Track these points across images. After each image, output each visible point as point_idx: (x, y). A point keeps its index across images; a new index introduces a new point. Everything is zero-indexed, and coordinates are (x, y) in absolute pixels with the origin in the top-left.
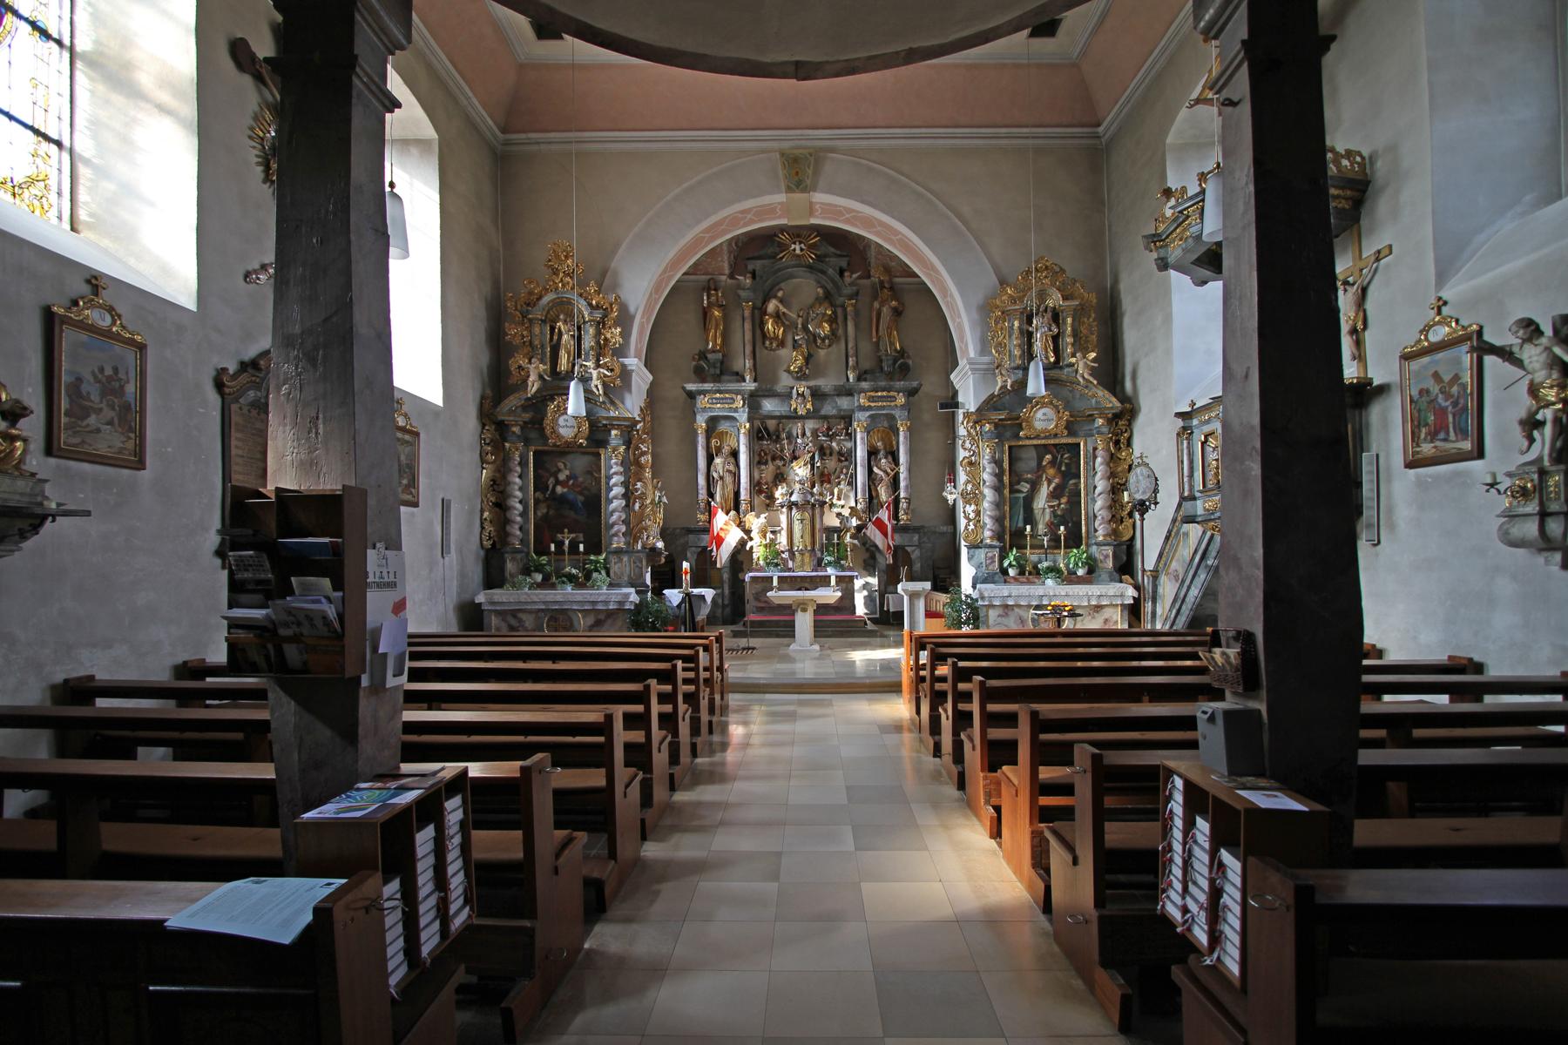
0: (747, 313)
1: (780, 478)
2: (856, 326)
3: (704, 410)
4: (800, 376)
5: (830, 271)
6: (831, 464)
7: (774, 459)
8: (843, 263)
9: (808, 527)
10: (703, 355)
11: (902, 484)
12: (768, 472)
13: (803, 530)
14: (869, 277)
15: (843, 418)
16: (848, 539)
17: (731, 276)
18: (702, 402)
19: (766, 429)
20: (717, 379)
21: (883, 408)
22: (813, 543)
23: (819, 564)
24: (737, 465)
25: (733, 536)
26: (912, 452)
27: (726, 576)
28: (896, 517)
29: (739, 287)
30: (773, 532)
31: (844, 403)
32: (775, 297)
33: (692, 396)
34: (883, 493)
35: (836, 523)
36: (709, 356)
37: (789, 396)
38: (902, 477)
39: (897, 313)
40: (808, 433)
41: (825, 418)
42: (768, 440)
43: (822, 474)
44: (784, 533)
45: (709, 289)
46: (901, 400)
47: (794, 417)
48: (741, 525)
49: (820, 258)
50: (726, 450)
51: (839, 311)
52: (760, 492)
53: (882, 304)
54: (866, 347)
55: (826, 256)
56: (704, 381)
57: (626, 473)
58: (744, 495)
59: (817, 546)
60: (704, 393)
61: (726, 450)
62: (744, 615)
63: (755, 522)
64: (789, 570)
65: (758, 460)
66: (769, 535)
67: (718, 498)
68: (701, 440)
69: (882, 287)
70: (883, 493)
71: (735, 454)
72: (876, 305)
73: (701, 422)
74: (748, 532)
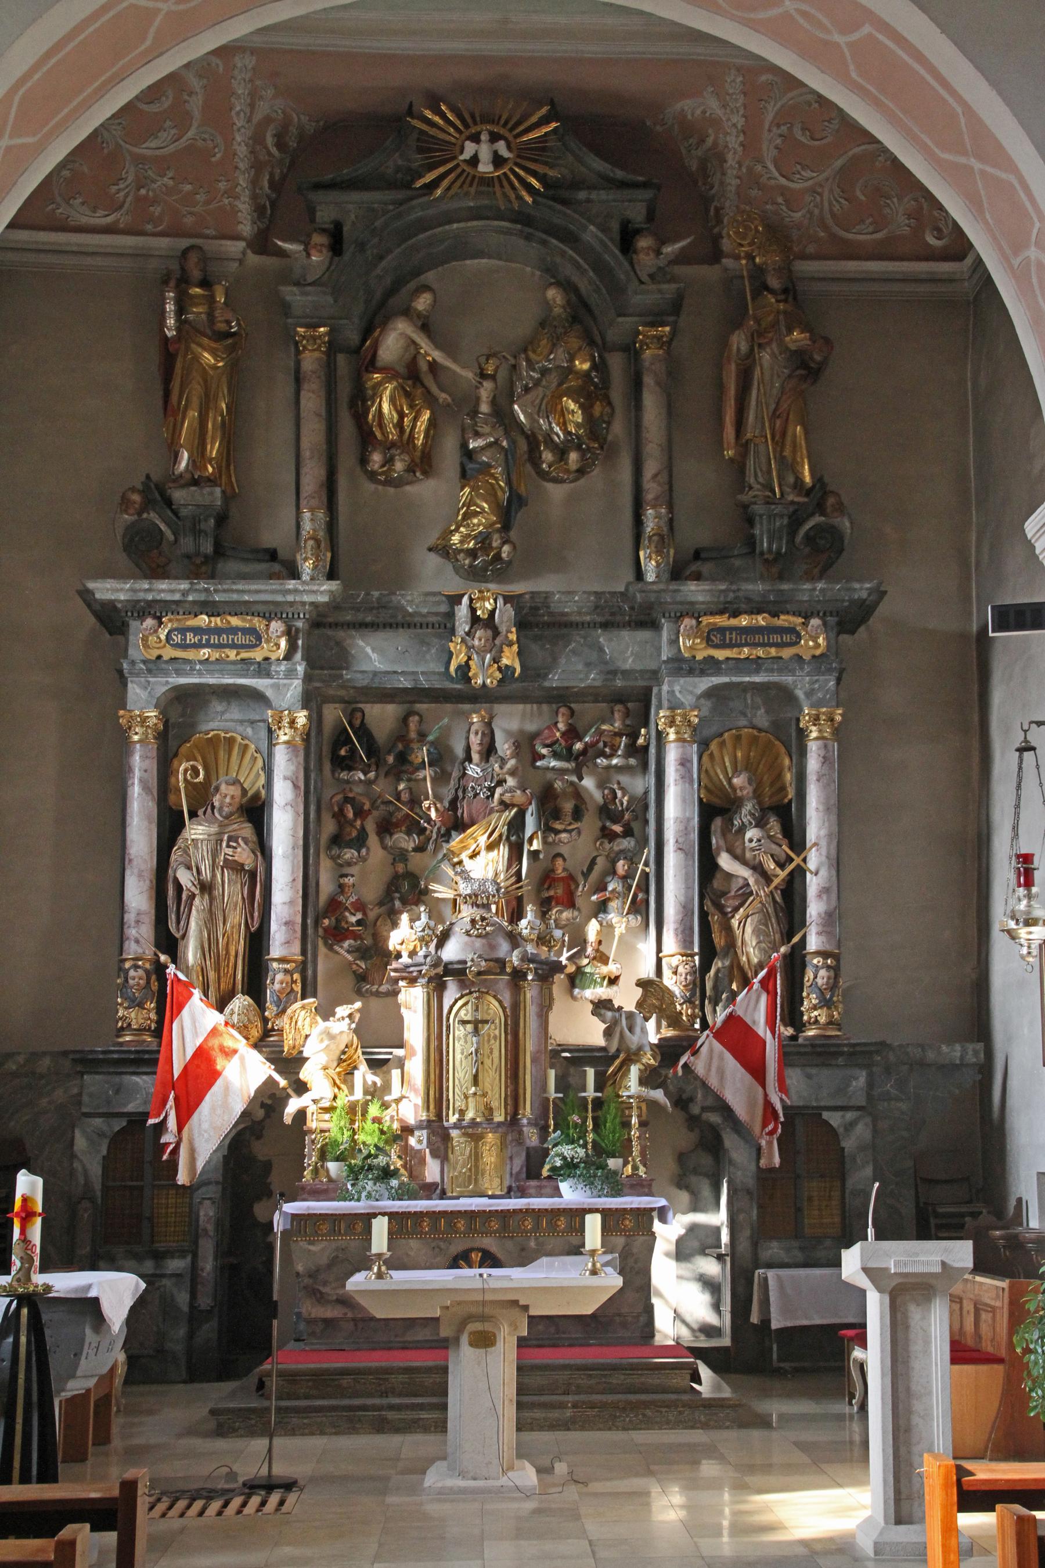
0: (310, 361)
1: (407, 890)
2: (671, 411)
3: (155, 666)
4: (483, 565)
5: (591, 234)
6: (577, 844)
7: (386, 828)
8: (637, 213)
9: (497, 1052)
10: (157, 494)
11: (815, 909)
12: (369, 869)
13: (478, 1056)
14: (715, 256)
15: (619, 698)
16: (632, 1085)
17: (261, 244)
18: (149, 639)
20: (203, 567)
21: (756, 664)
22: (514, 1100)
23: (533, 1171)
24: (263, 848)
25: (245, 1073)
26: (844, 810)
27: (207, 1213)
28: (793, 1016)
29: (286, 277)
30: (375, 1065)
31: (626, 649)
32: (407, 312)
33: (113, 621)
34: (751, 939)
35: (592, 1033)
36: (179, 495)
37: (446, 626)
38: (813, 884)
39: (807, 368)
40: (504, 747)
41: (561, 698)
42: (373, 777)
43: (546, 878)
44: (416, 1067)
45: (183, 282)
46: (815, 640)
47: (463, 694)
48: (266, 1040)
49: (556, 191)
50: (226, 796)
51: (616, 362)
52: (337, 934)
53: (757, 341)
54: (700, 478)
55: (576, 184)
56: (158, 572)
58: (281, 942)
59: (527, 1111)
60: (155, 610)
61: (226, 796)
62: (263, 1348)
63: (321, 1036)
64: (430, 1190)
65: (333, 829)
66: (363, 1076)
67: (191, 953)
68: (141, 764)
69: (761, 287)
70: (751, 939)
71: (255, 812)
72: (739, 342)
73: (143, 702)
74: (289, 1063)
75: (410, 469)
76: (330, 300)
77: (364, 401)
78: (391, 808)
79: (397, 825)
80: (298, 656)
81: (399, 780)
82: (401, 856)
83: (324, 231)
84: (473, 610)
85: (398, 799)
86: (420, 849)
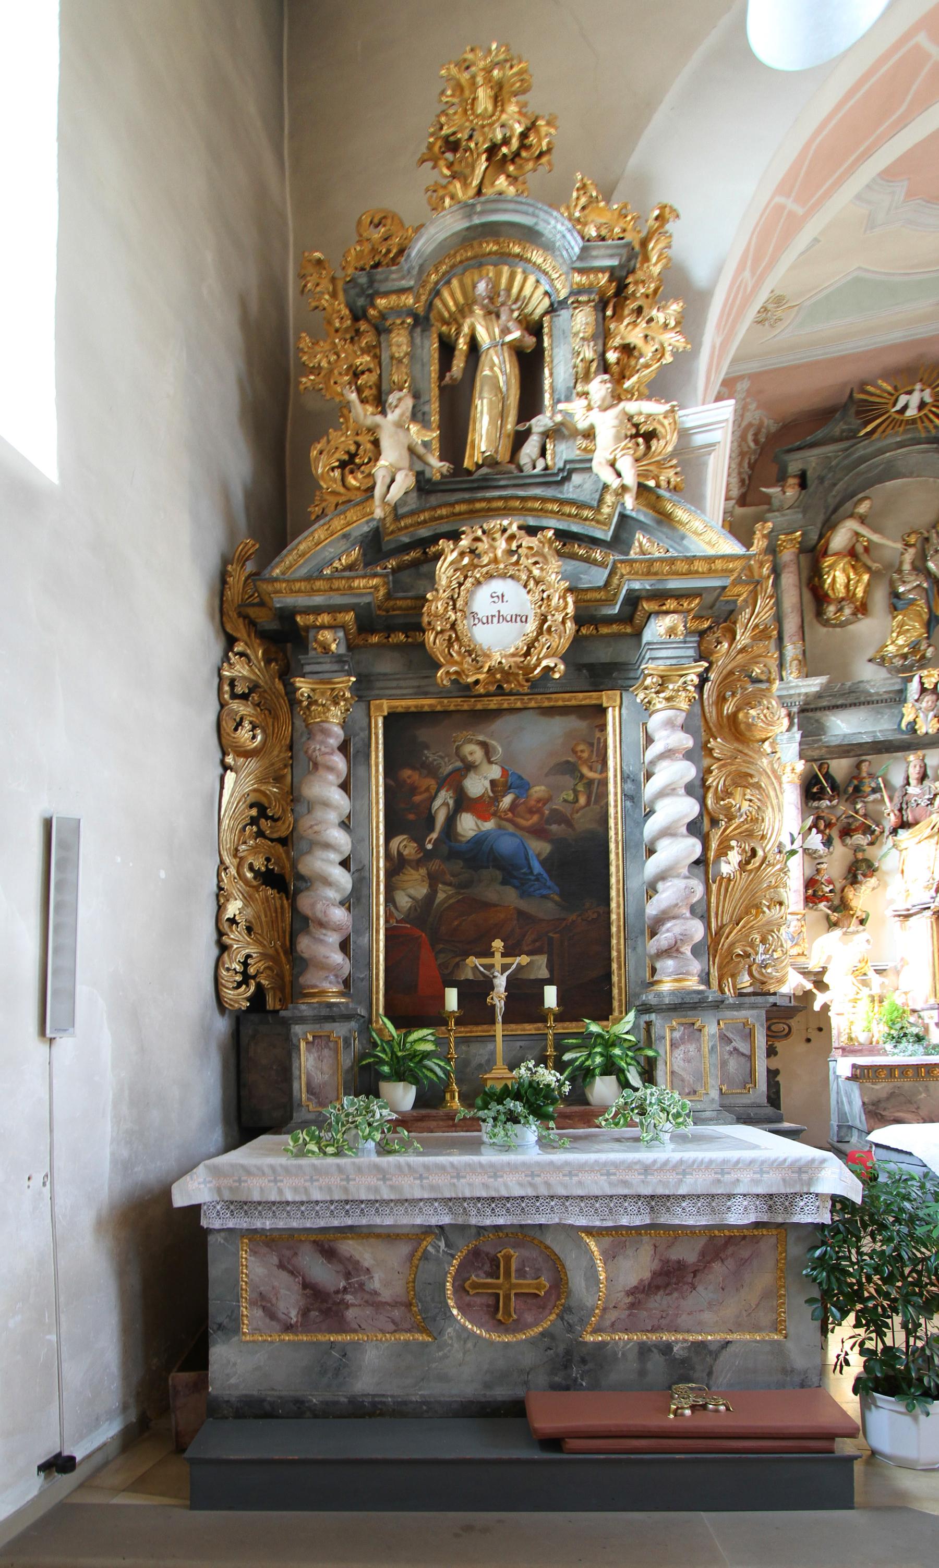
19: (827, 776)
57: (700, 752)
75: (854, 614)
76: (800, 516)
77: (820, 576)
78: (851, 820)
79: (856, 830)
80: (795, 728)
81: (855, 803)
82: (857, 849)
83: (795, 476)
84: (922, 684)
85: (857, 813)
86: (871, 844)
